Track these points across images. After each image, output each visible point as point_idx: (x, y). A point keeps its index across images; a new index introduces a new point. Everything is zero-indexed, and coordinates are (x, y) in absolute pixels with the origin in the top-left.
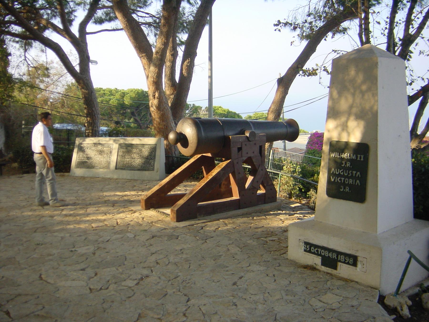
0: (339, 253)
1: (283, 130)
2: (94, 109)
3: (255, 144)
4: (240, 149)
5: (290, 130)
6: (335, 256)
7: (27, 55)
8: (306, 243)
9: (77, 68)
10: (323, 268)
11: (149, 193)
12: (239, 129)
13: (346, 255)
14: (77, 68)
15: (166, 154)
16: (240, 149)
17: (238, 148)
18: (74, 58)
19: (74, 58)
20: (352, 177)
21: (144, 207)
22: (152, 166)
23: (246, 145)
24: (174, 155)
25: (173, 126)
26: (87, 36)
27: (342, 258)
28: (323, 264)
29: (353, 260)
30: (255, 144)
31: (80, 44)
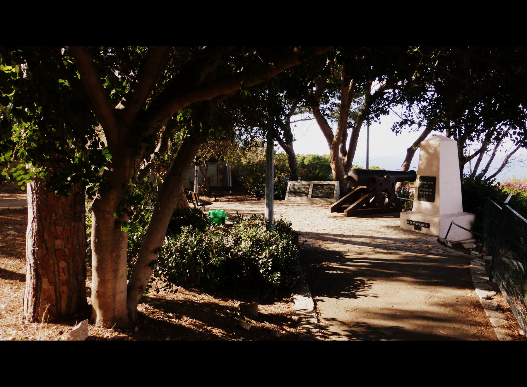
0: (421, 223)
4: (381, 184)
5: (411, 176)
6: (420, 224)
8: (408, 220)
10: (415, 231)
11: (333, 205)
13: (424, 223)
16: (381, 184)
20: (428, 192)
27: (422, 225)
28: (415, 229)
29: (427, 226)
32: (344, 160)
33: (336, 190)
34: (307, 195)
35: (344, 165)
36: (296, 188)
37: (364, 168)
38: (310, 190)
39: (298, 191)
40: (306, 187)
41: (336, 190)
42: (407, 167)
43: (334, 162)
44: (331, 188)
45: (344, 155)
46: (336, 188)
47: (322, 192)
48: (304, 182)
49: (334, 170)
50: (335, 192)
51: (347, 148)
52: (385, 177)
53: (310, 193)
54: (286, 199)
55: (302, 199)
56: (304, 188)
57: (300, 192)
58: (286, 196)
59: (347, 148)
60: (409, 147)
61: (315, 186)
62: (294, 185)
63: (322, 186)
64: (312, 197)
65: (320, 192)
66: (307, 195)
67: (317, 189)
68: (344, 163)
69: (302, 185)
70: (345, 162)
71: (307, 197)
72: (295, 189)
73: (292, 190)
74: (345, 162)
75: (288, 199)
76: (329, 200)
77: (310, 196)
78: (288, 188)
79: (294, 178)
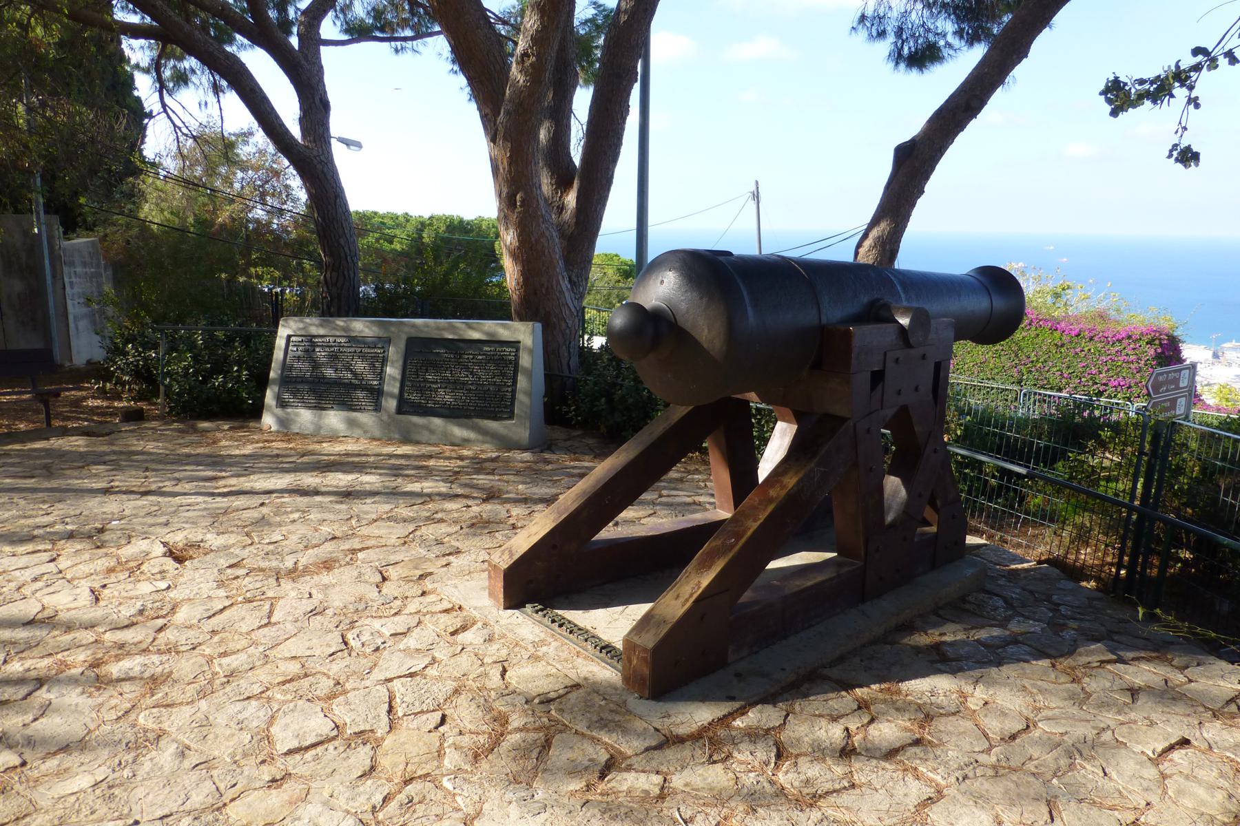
1: (978, 304)
2: (342, 241)
3: (924, 357)
4: (877, 378)
7: (167, 99)
9: (295, 131)
11: (523, 542)
12: (865, 299)
14: (295, 131)
15: (545, 369)
16: (877, 378)
17: (873, 373)
18: (286, 103)
19: (286, 103)
21: (501, 596)
22: (506, 407)
23: (897, 360)
24: (566, 373)
25: (564, 289)
26: (323, 49)
30: (924, 357)
31: (305, 75)
32: (561, 208)
33: (529, 374)
35: (562, 235)
36: (321, 354)
38: (393, 371)
39: (329, 373)
40: (375, 353)
41: (529, 374)
42: (889, 246)
44: (502, 358)
45: (563, 183)
46: (525, 360)
47: (455, 385)
48: (361, 326)
49: (514, 256)
50: (522, 382)
51: (576, 154)
52: (904, 321)
53: (392, 387)
54: (268, 420)
55: (352, 423)
56: (363, 357)
57: (337, 383)
58: (270, 397)
59: (576, 154)
60: (906, 136)
61: (418, 349)
62: (311, 338)
63: (459, 346)
64: (404, 407)
65: (447, 383)
66: (376, 394)
67: (436, 366)
68: (560, 228)
69: (352, 340)
70: (568, 215)
71: (378, 408)
72: (315, 365)
73: (303, 367)
75: (283, 422)
77: (391, 404)
78: (278, 354)
79: (338, 301)
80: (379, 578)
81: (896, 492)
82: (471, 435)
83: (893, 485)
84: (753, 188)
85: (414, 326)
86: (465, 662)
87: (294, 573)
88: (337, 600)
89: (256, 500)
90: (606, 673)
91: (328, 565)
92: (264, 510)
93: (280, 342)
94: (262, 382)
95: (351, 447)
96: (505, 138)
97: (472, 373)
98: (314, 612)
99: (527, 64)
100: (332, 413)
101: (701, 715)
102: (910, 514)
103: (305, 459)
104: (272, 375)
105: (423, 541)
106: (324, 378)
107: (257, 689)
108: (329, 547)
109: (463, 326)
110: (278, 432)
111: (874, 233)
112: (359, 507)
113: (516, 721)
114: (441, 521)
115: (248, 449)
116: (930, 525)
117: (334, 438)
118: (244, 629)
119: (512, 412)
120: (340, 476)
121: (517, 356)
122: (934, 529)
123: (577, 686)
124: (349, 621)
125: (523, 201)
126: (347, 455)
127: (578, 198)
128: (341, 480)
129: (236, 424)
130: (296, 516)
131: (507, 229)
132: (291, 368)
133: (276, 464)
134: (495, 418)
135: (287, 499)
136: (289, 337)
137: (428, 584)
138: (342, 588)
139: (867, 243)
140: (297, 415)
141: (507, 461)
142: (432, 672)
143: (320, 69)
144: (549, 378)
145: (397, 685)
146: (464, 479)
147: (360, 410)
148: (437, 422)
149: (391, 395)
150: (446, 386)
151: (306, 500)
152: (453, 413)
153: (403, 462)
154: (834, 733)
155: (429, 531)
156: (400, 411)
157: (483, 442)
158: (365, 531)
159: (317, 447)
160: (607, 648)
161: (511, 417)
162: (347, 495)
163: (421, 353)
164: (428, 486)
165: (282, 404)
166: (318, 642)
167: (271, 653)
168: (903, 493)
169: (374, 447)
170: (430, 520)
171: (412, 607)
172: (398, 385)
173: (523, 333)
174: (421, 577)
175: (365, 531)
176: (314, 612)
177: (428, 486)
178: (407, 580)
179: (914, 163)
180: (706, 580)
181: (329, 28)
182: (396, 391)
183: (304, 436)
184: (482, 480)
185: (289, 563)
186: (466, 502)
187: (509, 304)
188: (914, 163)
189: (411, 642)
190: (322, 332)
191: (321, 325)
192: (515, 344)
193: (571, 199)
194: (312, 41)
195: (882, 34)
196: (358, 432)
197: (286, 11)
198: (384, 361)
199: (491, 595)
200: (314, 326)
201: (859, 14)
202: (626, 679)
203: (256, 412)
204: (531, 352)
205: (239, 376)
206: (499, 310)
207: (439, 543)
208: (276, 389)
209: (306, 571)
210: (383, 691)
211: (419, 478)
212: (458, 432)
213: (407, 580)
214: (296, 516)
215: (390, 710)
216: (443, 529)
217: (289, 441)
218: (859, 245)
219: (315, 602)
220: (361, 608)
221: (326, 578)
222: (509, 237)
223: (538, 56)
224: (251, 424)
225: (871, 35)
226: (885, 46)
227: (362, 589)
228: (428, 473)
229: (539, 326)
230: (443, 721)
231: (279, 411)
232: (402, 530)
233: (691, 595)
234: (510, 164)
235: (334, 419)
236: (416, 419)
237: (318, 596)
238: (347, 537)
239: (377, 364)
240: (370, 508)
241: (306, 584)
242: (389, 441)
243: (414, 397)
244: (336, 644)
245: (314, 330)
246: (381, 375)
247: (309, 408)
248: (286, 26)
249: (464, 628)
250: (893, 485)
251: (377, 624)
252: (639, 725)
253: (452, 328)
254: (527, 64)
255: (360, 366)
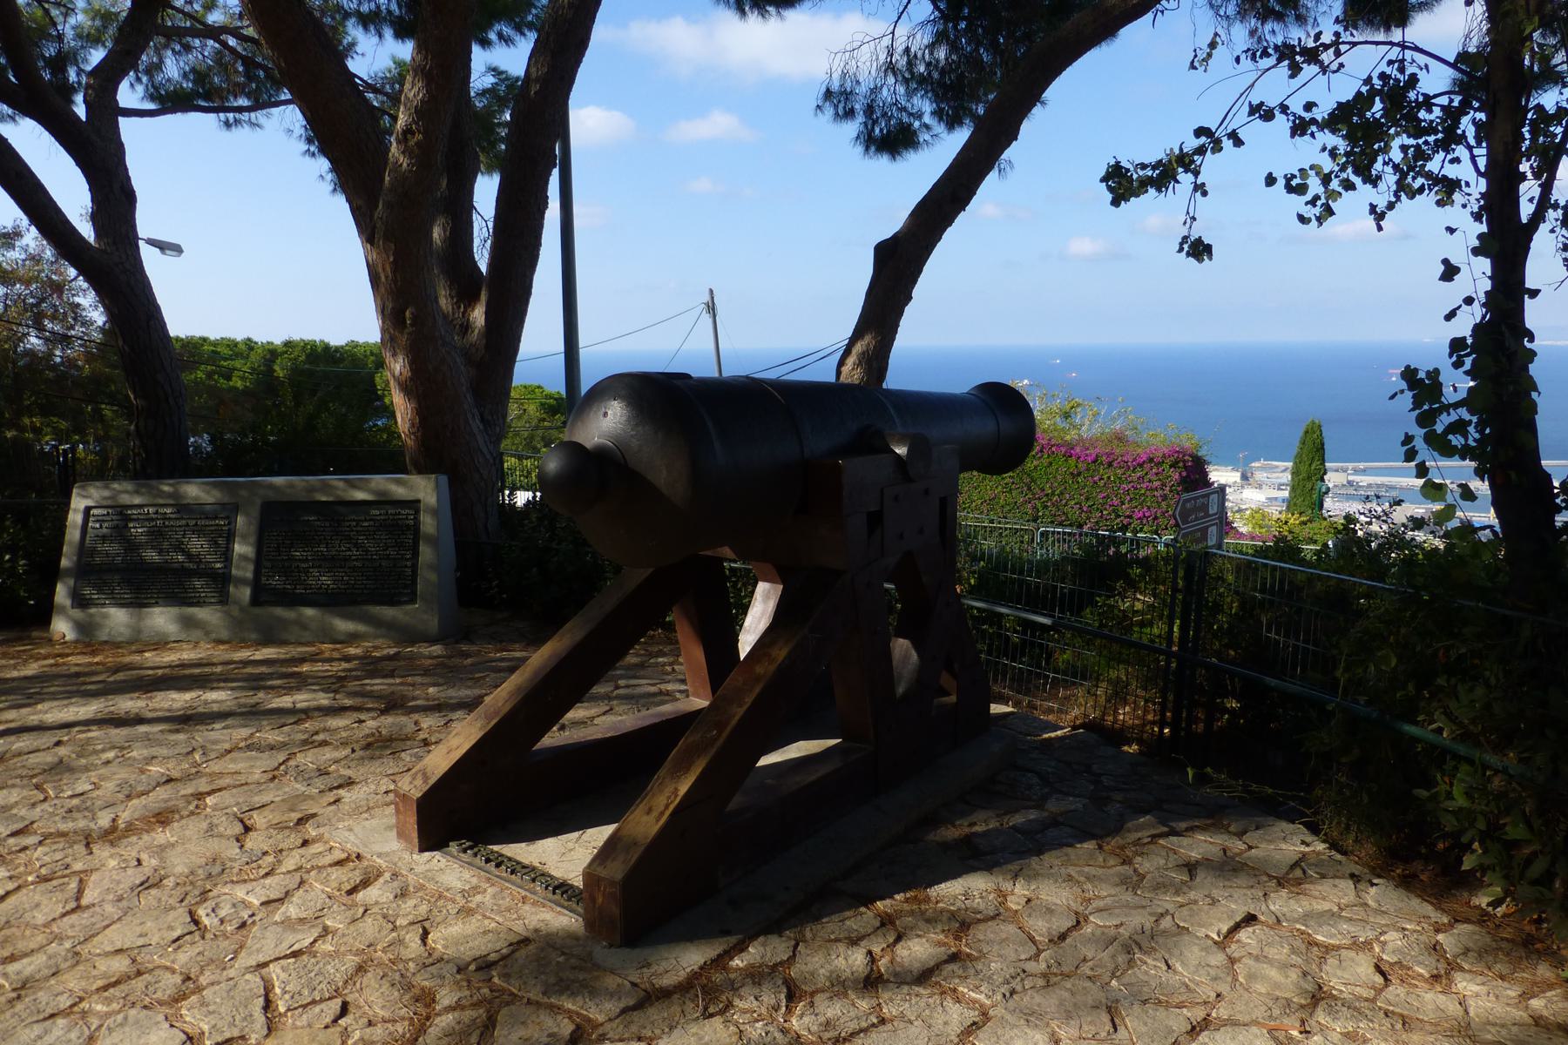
1: (983, 427)
3: (927, 492)
9: (86, 230)
11: (440, 761)
14: (86, 230)
16: (875, 520)
21: (415, 835)
25: (476, 431)
30: (927, 492)
32: (466, 327)
33: (434, 541)
34: (221, 582)
36: (137, 530)
37: (716, 375)
39: (152, 555)
41: (434, 541)
42: (876, 362)
43: (403, 339)
44: (398, 521)
46: (428, 524)
48: (194, 491)
49: (406, 388)
50: (426, 553)
51: (482, 259)
52: (901, 450)
54: (62, 627)
55: (188, 623)
56: (199, 531)
58: (61, 594)
59: (482, 259)
60: (887, 233)
62: (122, 514)
66: (221, 582)
69: (185, 509)
70: (474, 336)
71: (224, 599)
72: (131, 546)
74: (474, 336)
76: (388, 612)
78: (73, 534)
79: (159, 458)
80: (239, 828)
81: (906, 657)
82: (361, 628)
83: (901, 647)
84: (707, 298)
85: (271, 486)
86: (369, 927)
87: (112, 835)
88: (179, 865)
89: (47, 739)
90: (562, 920)
91: (163, 818)
92: (62, 751)
93: (75, 518)
94: (49, 574)
95: (187, 655)
96: (386, 238)
97: (356, 545)
98: (146, 885)
99: (412, 143)
100: (157, 610)
101: (691, 958)
102: (925, 683)
103: (120, 676)
104: (65, 563)
105: (300, 773)
106: (143, 562)
107: (64, 1002)
108: (162, 793)
109: (341, 484)
110: (76, 642)
111: (859, 347)
112: (201, 735)
113: (446, 997)
114: (324, 743)
115: (32, 669)
116: (949, 694)
117: (161, 644)
118: (40, 918)
119: (414, 593)
120: (174, 695)
121: (416, 519)
122: (953, 698)
123: (525, 941)
124: (199, 889)
125: (415, 317)
126: (183, 665)
127: (486, 313)
128: (177, 700)
129: (11, 635)
130: (111, 755)
131: (394, 355)
132: (93, 552)
133: (76, 686)
134: (392, 602)
135: (95, 733)
136: (88, 510)
137: (311, 831)
138: (185, 848)
139: (850, 361)
140: (106, 616)
141: (411, 658)
142: (326, 946)
143: (120, 147)
144: (461, 547)
145: (275, 971)
146: (353, 685)
147: (198, 604)
148: (309, 612)
149: (243, 581)
150: (316, 569)
151: (123, 732)
152: (331, 601)
153: (263, 669)
154: (856, 960)
155: (307, 759)
156: (256, 601)
157: (376, 637)
158: (215, 767)
159: (136, 658)
160: (562, 888)
161: (413, 601)
162: (186, 720)
163: (279, 520)
164: (302, 699)
165: (80, 601)
166: (154, 926)
167: (84, 950)
168: (914, 656)
169: (221, 653)
170: (308, 744)
171: (290, 863)
172: (251, 567)
173: (424, 489)
174: (301, 821)
175: (215, 767)
176: (146, 885)
177: (302, 699)
178: (280, 827)
179: (898, 264)
180: (683, 789)
181: (129, 94)
182: (249, 575)
183: (116, 645)
184: (378, 684)
185: (104, 820)
186: (356, 716)
187: (402, 454)
188: (898, 264)
189: (292, 910)
190: (137, 500)
191: (137, 492)
192: (414, 504)
193: (478, 315)
194: (106, 111)
195: (849, 114)
196: (196, 634)
197: (64, 71)
198: (230, 537)
199: (401, 835)
200: (128, 494)
201: (823, 89)
202: (590, 924)
203: (43, 614)
204: (435, 512)
205: (14, 568)
206: (391, 461)
207: (323, 773)
208: (71, 582)
209: (130, 829)
210: (254, 980)
211: (289, 690)
212: (343, 626)
213: (280, 827)
214: (111, 755)
215: (268, 1005)
216: (328, 754)
217: (94, 653)
218: (841, 363)
219: (147, 870)
220: (217, 871)
221: (161, 836)
222: (398, 366)
223: (425, 133)
224: (35, 634)
225: (837, 114)
226: (852, 128)
227: (214, 845)
228: (302, 682)
229: (444, 479)
230: (344, 1010)
231: (77, 614)
232: (269, 761)
233: (667, 807)
234: (394, 272)
235: (161, 619)
236: (279, 611)
237: (150, 862)
238: (187, 778)
239: (221, 541)
240: (220, 735)
241: (132, 847)
242: (243, 643)
243: (276, 581)
244: (178, 921)
245: (126, 499)
246: (227, 555)
247: (122, 605)
248: (68, 91)
249: (365, 883)
250: (901, 647)
251: (240, 892)
252: (611, 982)
253: (326, 487)
254: (412, 143)
255: (197, 544)
